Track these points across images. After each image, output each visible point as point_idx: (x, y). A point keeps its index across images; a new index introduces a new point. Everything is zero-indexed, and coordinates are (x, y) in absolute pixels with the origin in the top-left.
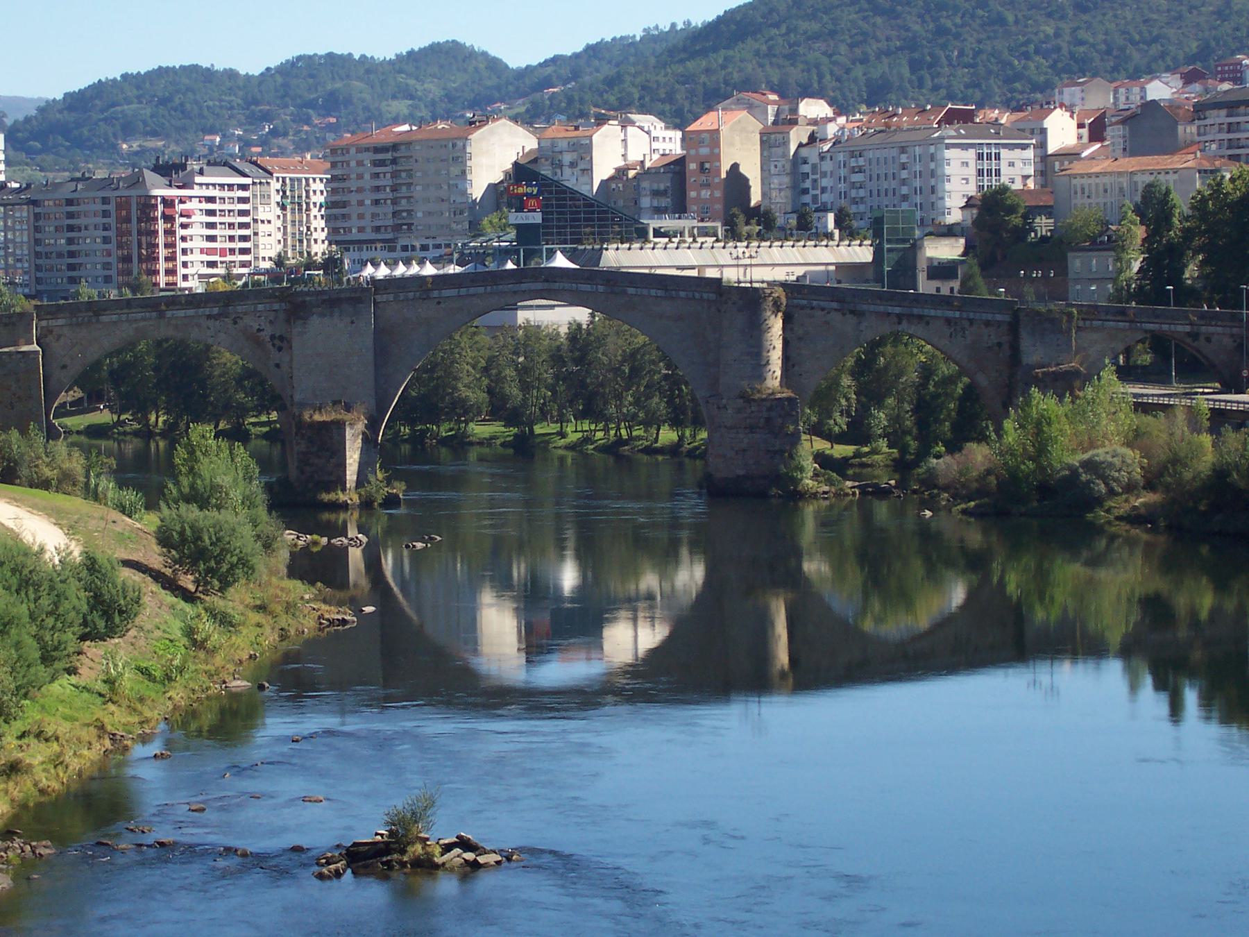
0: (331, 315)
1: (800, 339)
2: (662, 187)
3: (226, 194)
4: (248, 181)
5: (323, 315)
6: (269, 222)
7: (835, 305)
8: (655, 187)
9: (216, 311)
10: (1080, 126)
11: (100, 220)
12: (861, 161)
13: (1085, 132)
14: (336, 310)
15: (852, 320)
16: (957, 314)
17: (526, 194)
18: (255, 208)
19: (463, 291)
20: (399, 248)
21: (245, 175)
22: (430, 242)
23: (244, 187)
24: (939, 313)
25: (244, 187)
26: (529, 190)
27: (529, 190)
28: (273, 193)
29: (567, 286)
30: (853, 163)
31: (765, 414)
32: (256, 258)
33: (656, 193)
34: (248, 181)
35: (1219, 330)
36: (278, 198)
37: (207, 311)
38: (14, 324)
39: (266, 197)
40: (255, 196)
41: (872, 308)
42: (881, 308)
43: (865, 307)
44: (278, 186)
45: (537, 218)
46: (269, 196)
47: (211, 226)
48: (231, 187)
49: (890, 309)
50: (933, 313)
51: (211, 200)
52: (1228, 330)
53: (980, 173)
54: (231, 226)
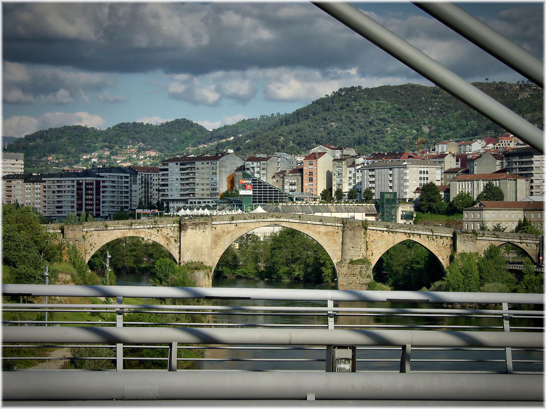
1: (372, 242)
2: (293, 181)
3: (120, 180)
4: (129, 175)
5: (192, 229)
6: (136, 191)
7: (385, 229)
8: (291, 181)
10: (457, 161)
12: (373, 173)
13: (459, 163)
17: (247, 183)
18: (131, 186)
20: (189, 202)
21: (128, 173)
22: (202, 201)
23: (127, 177)
24: (425, 233)
25: (127, 177)
26: (248, 182)
27: (248, 182)
28: (138, 180)
29: (285, 220)
30: (370, 173)
32: (131, 205)
33: (291, 184)
34: (129, 175)
35: (531, 241)
36: (140, 182)
37: (148, 226)
38: (74, 230)
39: (135, 182)
40: (131, 181)
42: (403, 231)
44: (140, 177)
45: (250, 193)
46: (136, 181)
47: (113, 192)
48: (121, 177)
49: (406, 231)
50: (422, 233)
51: (113, 182)
52: (534, 242)
53: (421, 178)
54: (121, 192)
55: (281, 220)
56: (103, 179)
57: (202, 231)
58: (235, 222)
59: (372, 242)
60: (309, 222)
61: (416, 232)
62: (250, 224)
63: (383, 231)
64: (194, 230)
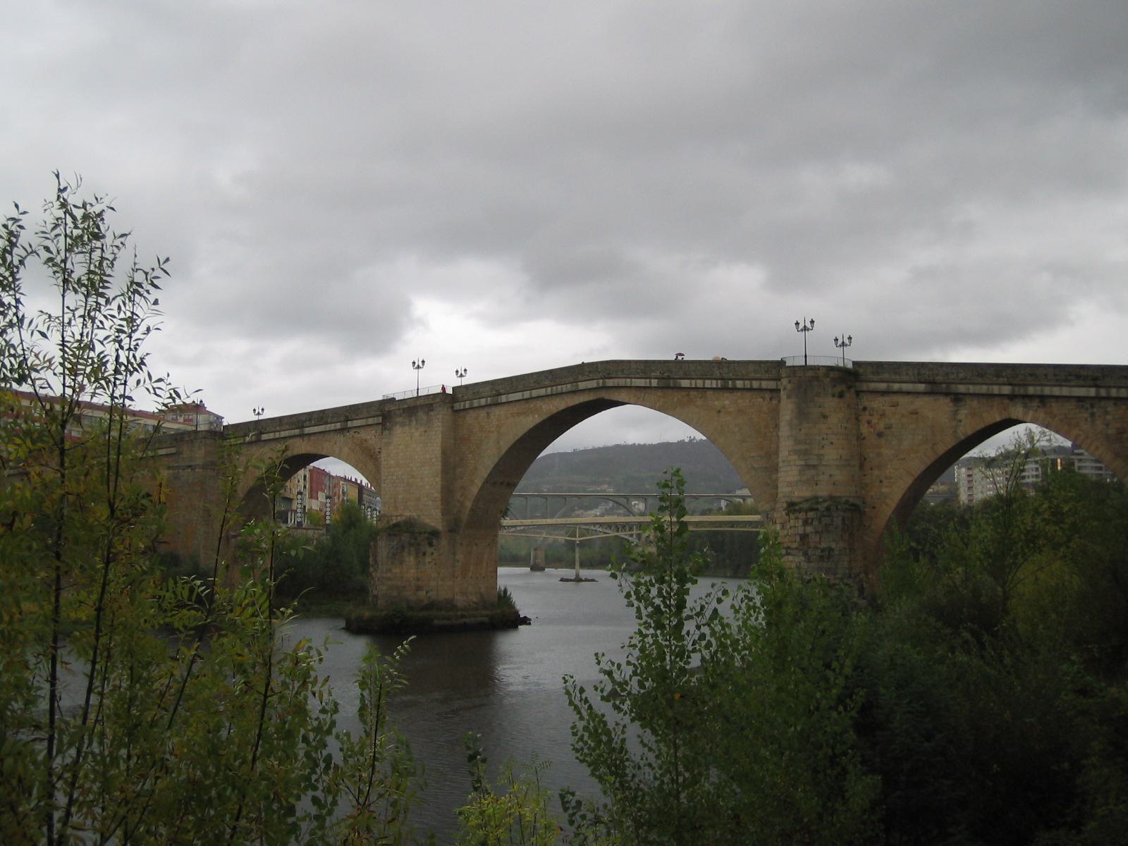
0: (409, 425)
1: (880, 435)
5: (403, 425)
7: (921, 387)
9: (338, 426)
11: (1034, 473)
14: (413, 418)
15: (945, 404)
16: (1092, 392)
19: (527, 395)
29: (622, 382)
31: (801, 530)
41: (972, 389)
42: (984, 389)
43: (962, 388)
49: (996, 389)
50: (1056, 391)
55: (610, 383)
56: (1080, 457)
57: (422, 429)
58: (504, 399)
59: (880, 435)
60: (685, 383)
61: (1031, 390)
62: (539, 403)
63: (918, 394)
64: (407, 428)
